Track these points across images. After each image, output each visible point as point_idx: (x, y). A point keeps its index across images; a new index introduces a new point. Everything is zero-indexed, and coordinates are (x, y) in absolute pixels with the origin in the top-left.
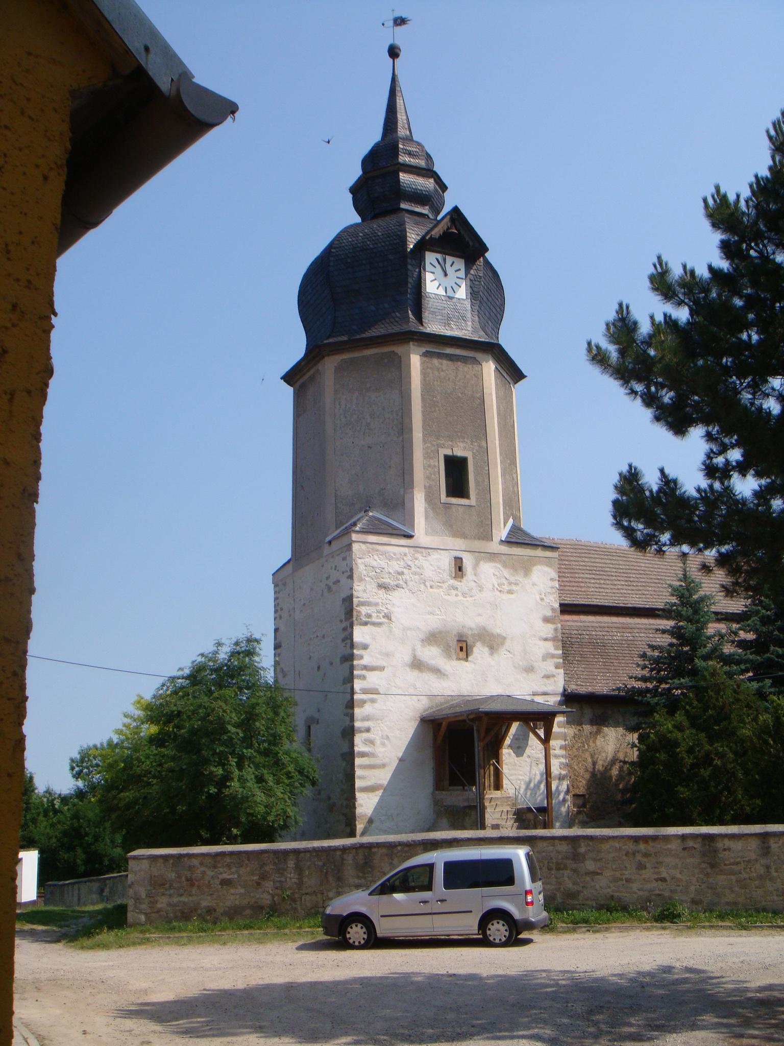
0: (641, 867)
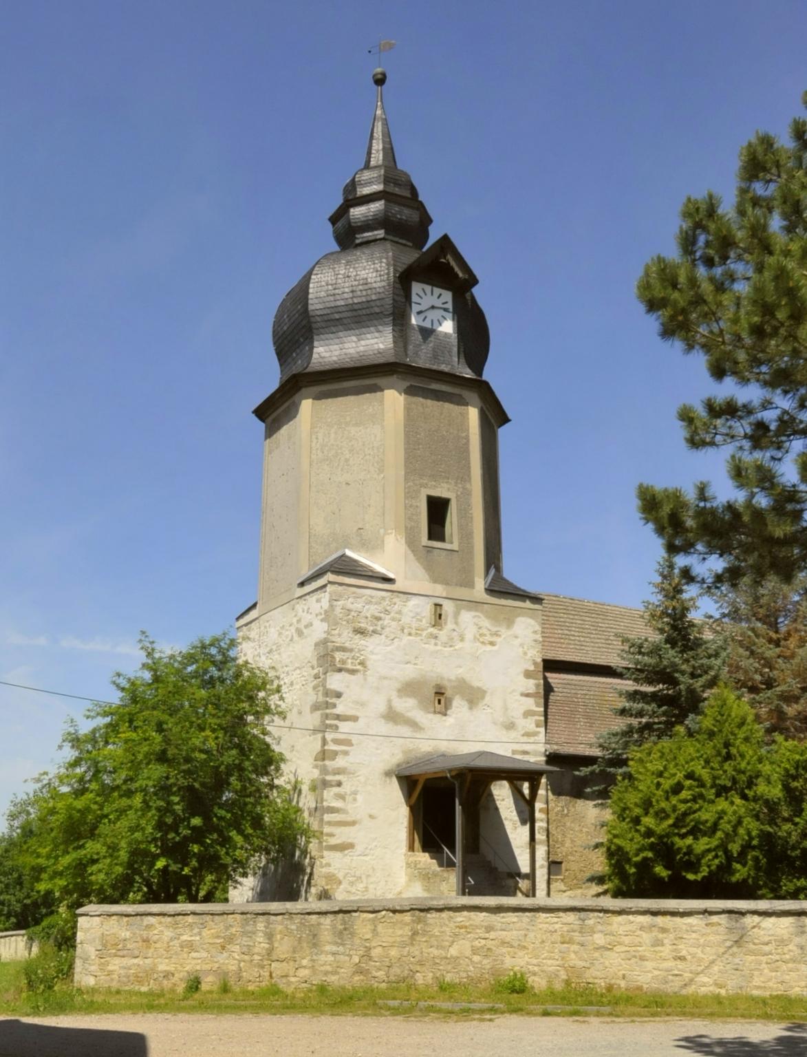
0: (658, 943)
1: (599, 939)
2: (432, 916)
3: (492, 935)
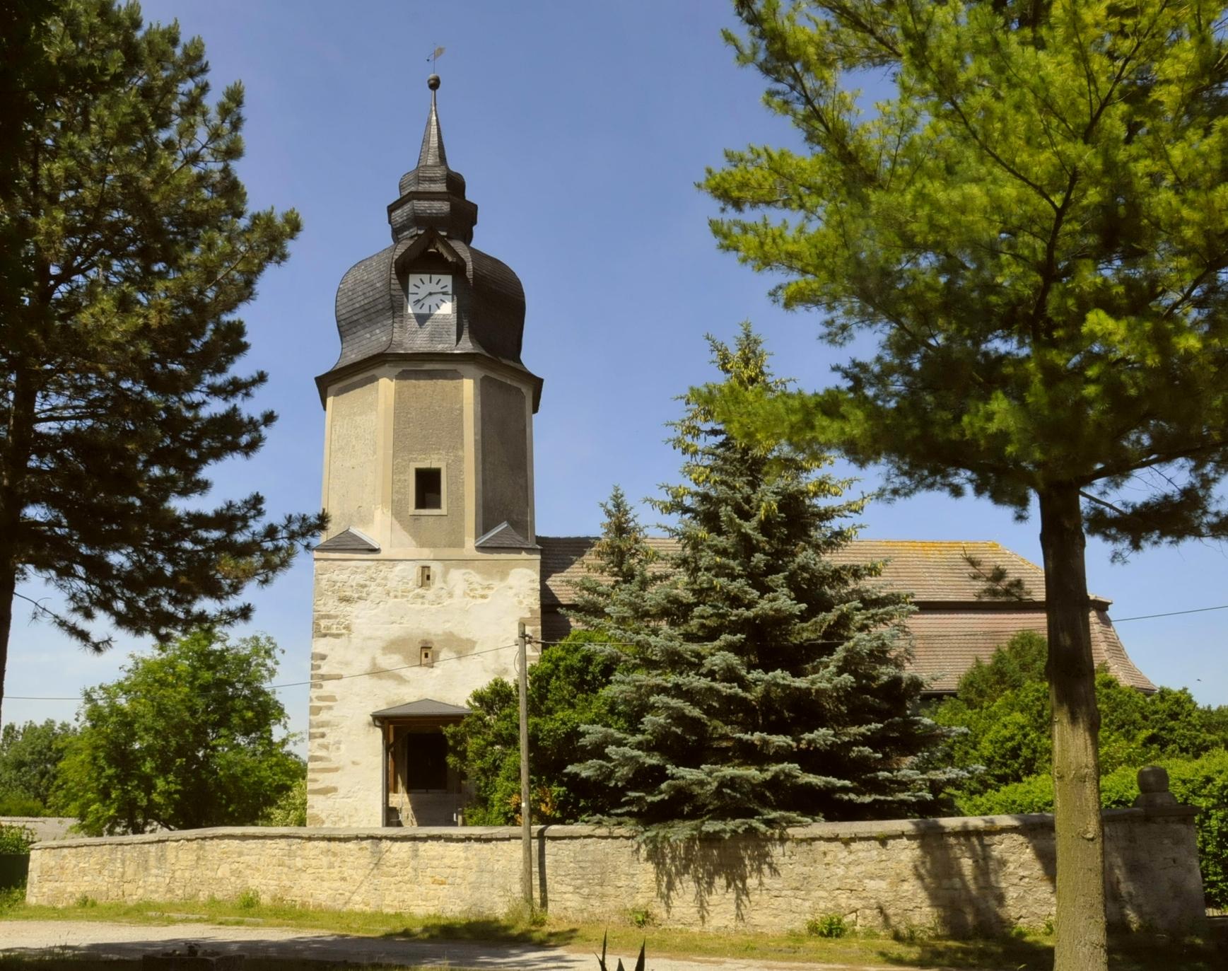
0: (331, 866)
1: (299, 863)
2: (208, 843)
3: (242, 859)
